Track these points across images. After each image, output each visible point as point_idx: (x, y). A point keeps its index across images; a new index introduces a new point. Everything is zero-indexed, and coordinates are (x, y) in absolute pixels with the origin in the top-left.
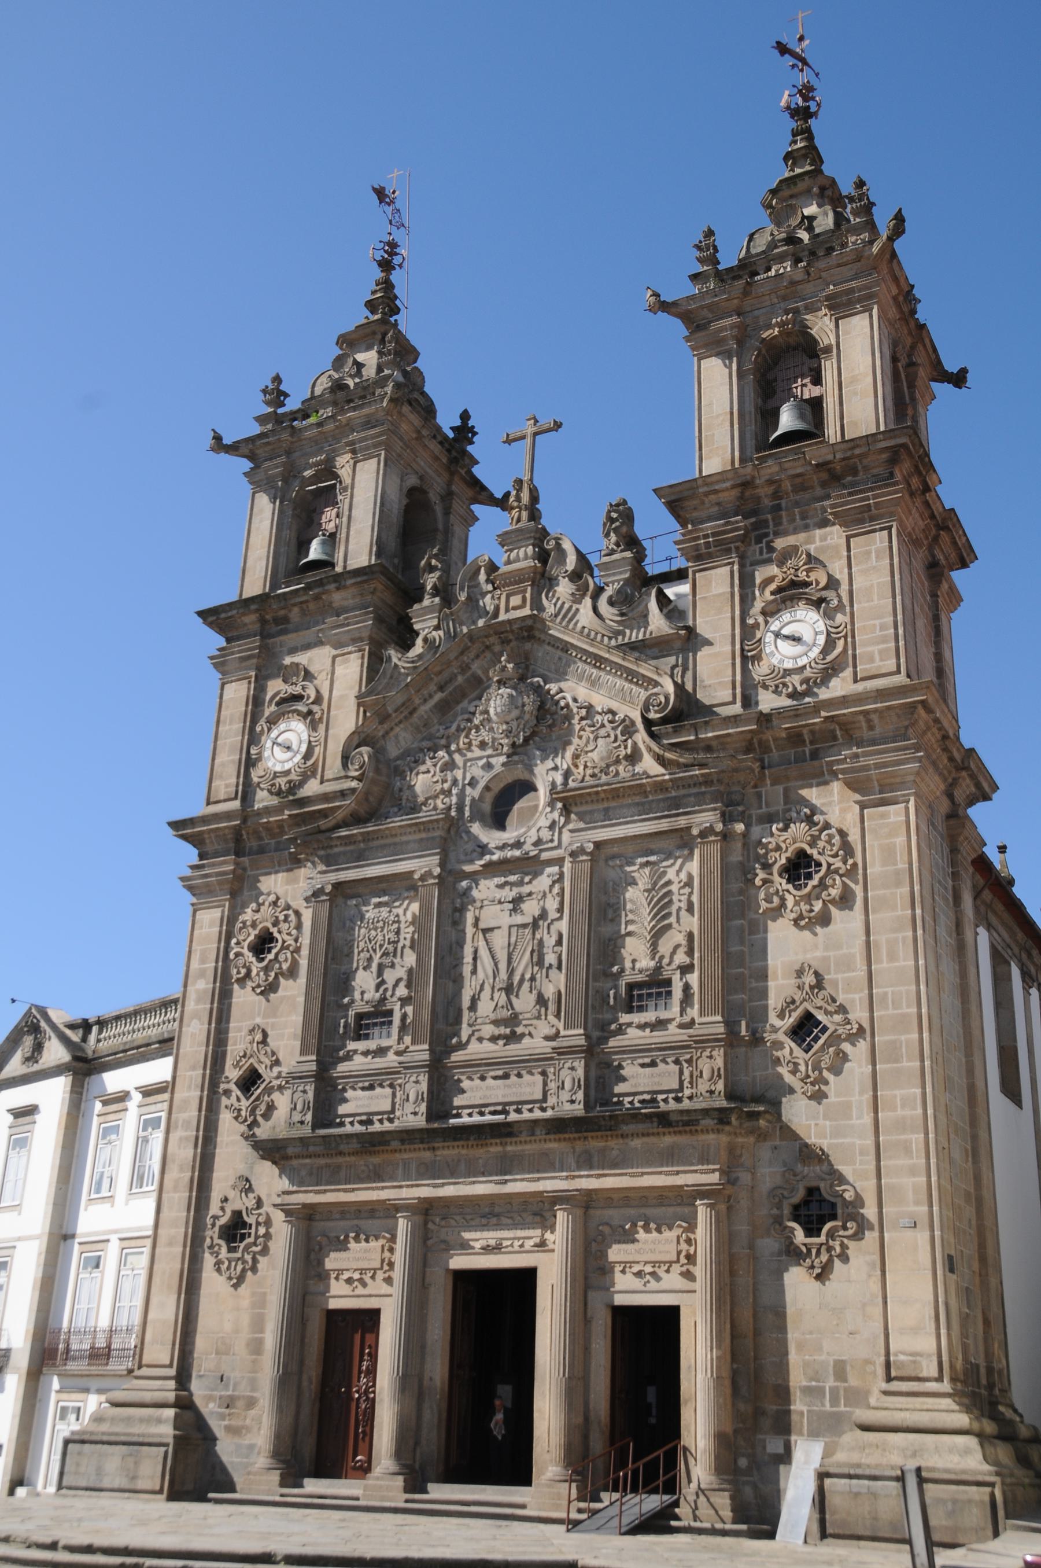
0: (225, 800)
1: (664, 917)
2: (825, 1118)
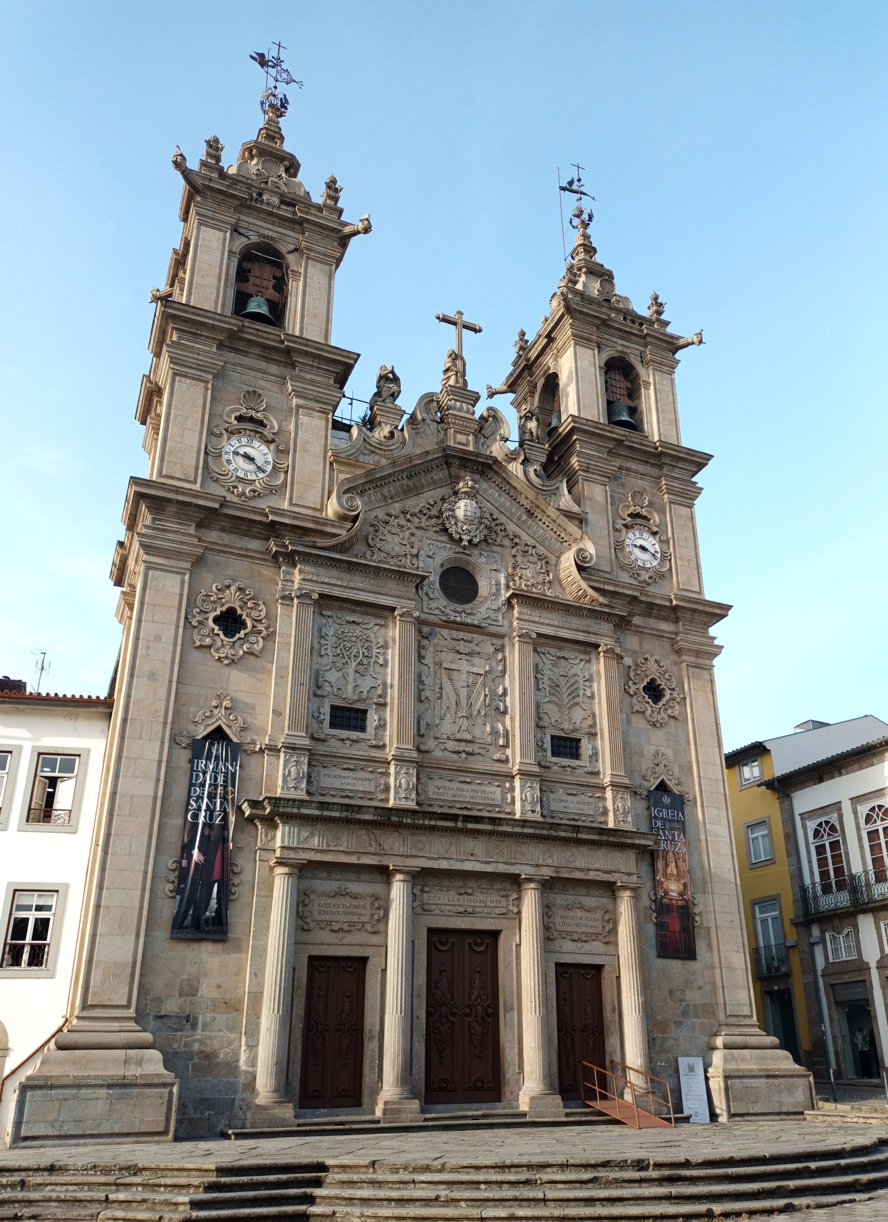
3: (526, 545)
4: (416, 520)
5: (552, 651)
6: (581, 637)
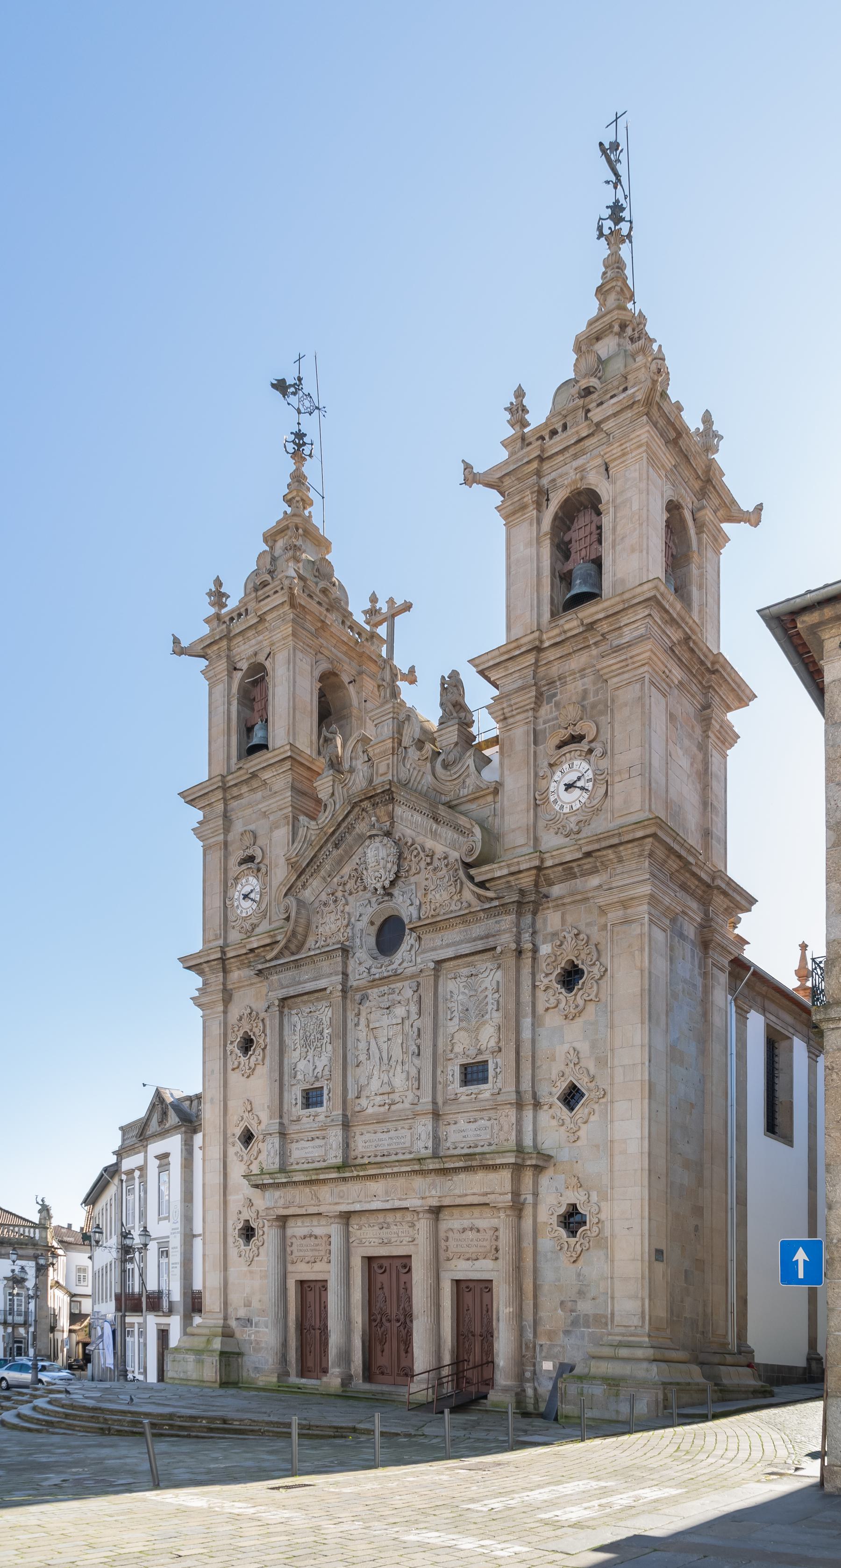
6: (480, 945)
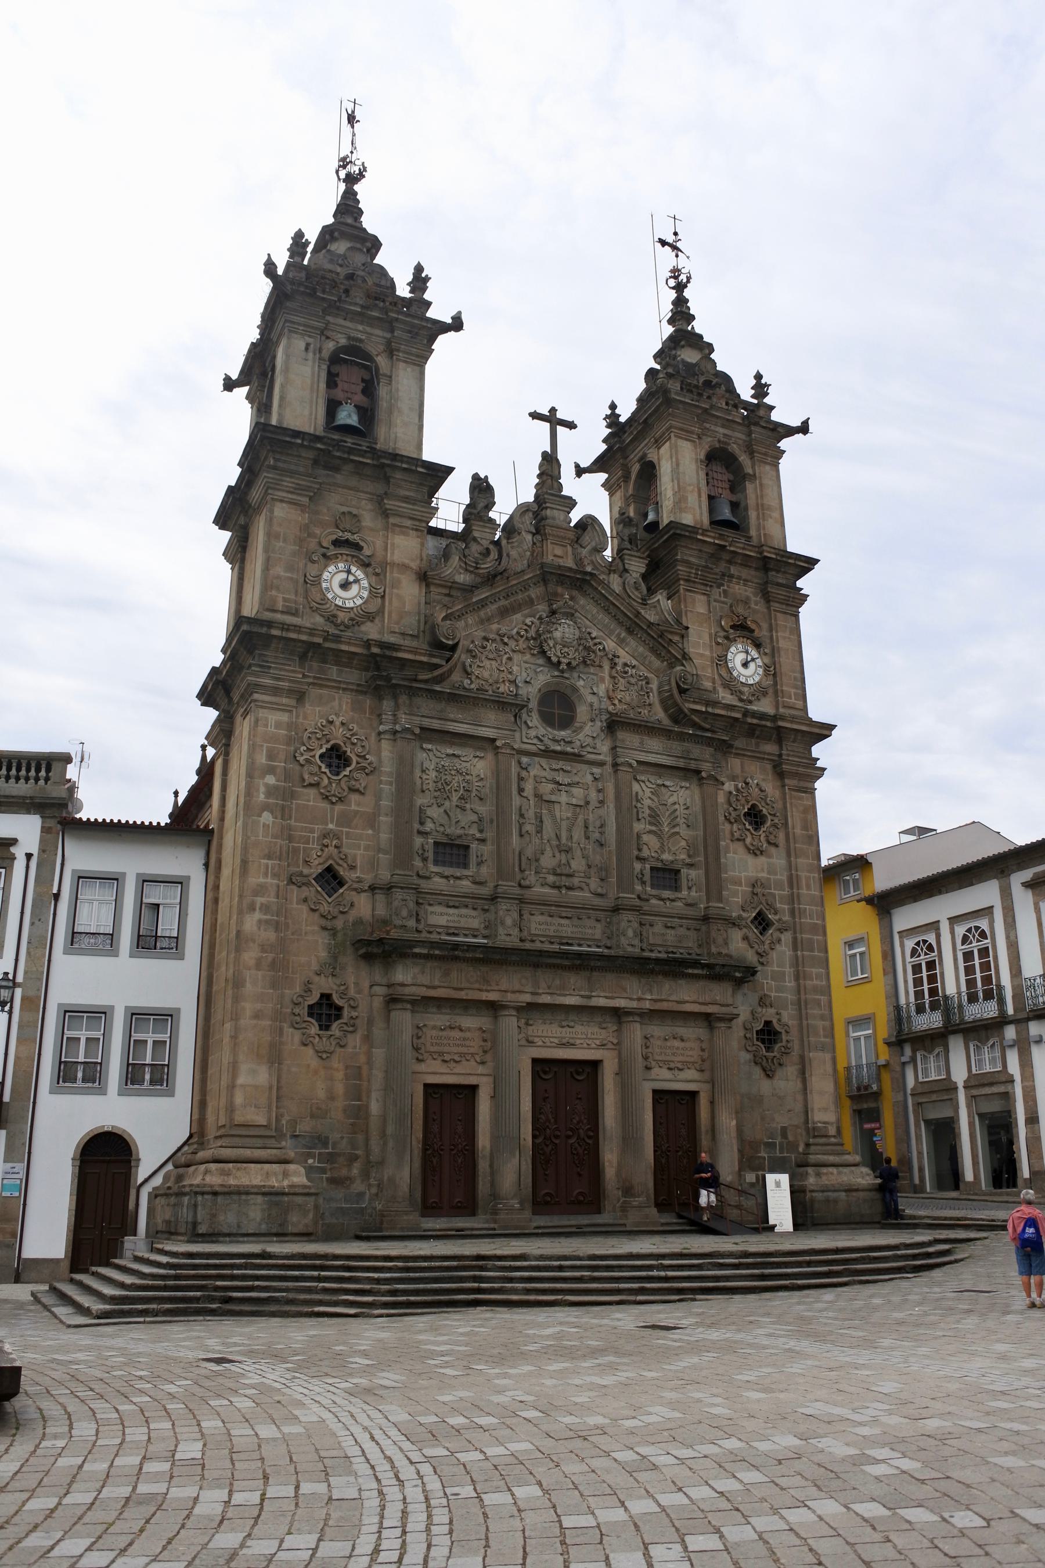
0: (282, 612)
1: (674, 826)
2: (772, 979)
3: (625, 665)
4: (512, 644)
5: (652, 779)
6: (681, 763)
